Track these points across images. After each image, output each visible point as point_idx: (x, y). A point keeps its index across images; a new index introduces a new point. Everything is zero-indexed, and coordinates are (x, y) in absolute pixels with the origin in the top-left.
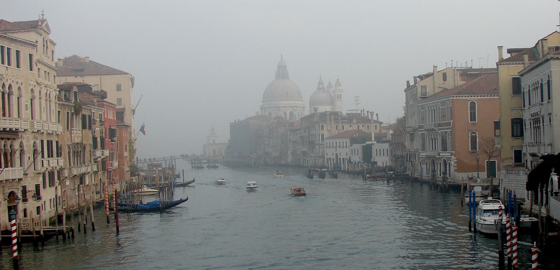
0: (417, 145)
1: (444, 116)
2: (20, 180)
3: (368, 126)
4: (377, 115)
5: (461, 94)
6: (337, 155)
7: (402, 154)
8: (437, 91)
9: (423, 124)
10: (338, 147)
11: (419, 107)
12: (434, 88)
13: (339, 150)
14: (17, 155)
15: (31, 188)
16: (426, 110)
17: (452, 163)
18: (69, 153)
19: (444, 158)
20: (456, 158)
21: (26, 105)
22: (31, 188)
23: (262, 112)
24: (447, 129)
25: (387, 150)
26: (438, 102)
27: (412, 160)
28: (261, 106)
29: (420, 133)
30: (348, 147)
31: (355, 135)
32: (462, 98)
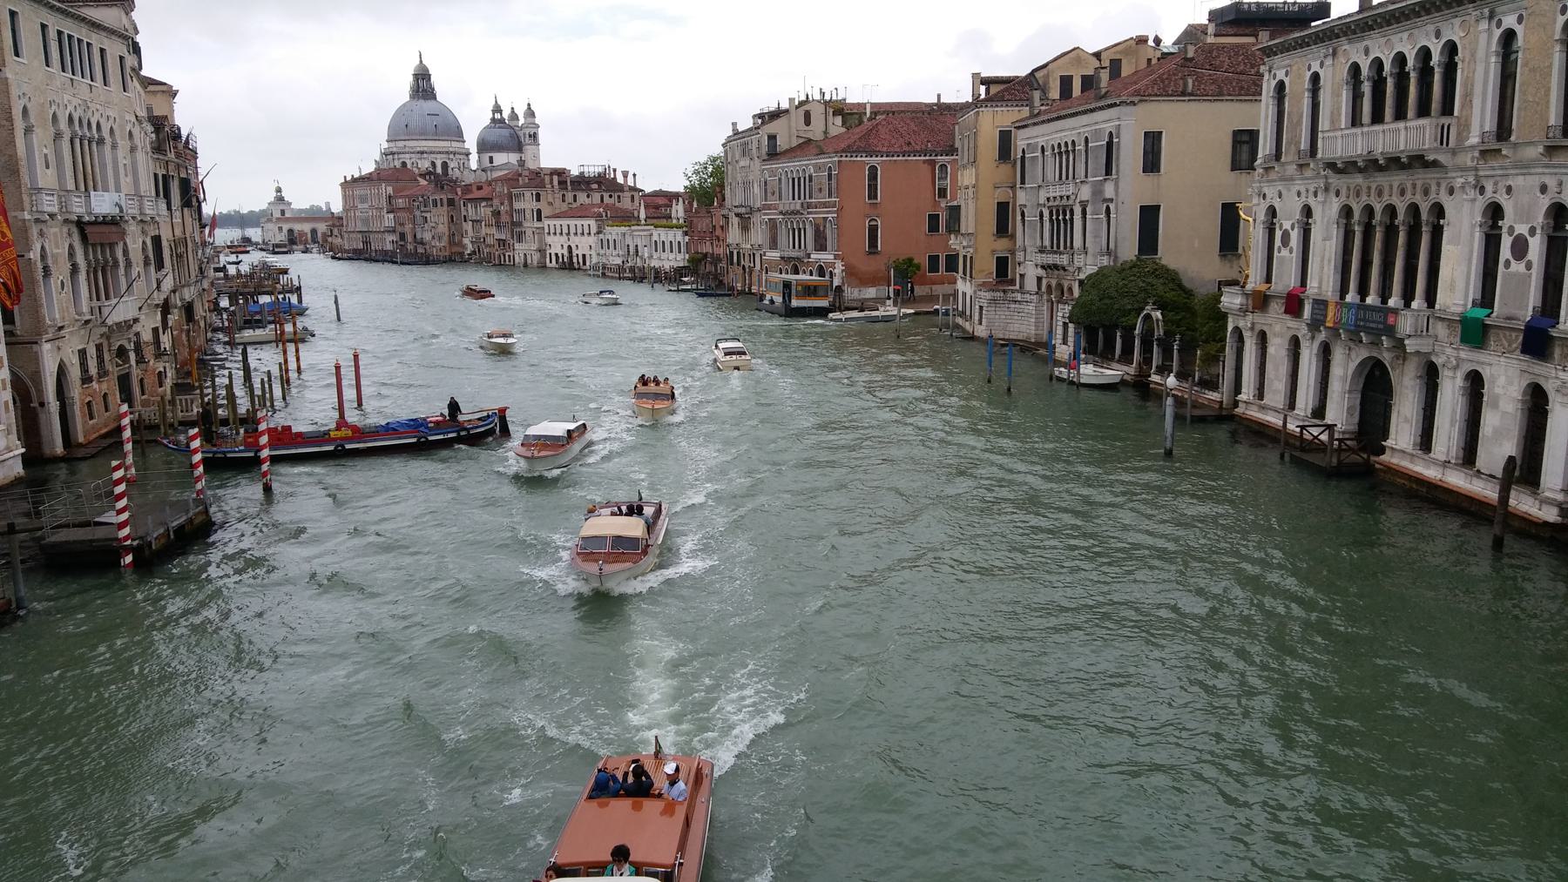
0: (758, 236)
1: (820, 190)
2: (136, 320)
3: (619, 197)
4: (634, 175)
5: (854, 152)
6: (570, 247)
10: (572, 234)
12: (790, 137)
13: (574, 241)
14: (122, 271)
15: (147, 336)
16: (780, 180)
17: (836, 271)
18: (172, 255)
21: (125, 165)
22: (147, 336)
26: (807, 165)
27: (742, 263)
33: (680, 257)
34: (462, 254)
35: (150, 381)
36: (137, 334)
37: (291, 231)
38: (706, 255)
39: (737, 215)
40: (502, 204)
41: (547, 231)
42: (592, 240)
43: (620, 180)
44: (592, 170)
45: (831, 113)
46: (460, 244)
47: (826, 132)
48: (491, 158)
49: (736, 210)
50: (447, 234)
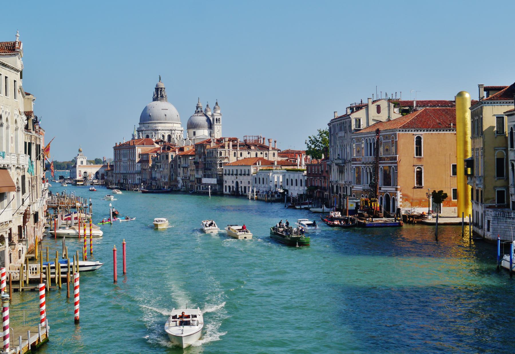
0: (349, 176)
3: (266, 154)
4: (275, 142)
6: (237, 183)
7: (320, 186)
8: (371, 123)
9: (358, 157)
11: (354, 139)
15: (15, 231)
19: (386, 193)
20: (401, 193)
23: (139, 134)
24: (392, 163)
25: (301, 180)
27: (339, 192)
28: (138, 128)
29: (354, 166)
30: (250, 175)
31: (257, 163)
32: (408, 133)
33: (301, 189)
34: (176, 186)
35: (15, 255)
36: (10, 229)
37: (85, 173)
38: (317, 187)
39: (336, 164)
40: (200, 158)
41: (224, 173)
42: (249, 178)
43: (266, 144)
44: (251, 140)
45: (393, 107)
46: (176, 179)
47: (389, 117)
48: (194, 134)
49: (336, 161)
50: (169, 175)
